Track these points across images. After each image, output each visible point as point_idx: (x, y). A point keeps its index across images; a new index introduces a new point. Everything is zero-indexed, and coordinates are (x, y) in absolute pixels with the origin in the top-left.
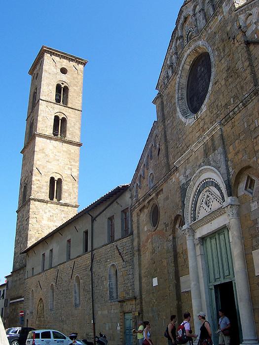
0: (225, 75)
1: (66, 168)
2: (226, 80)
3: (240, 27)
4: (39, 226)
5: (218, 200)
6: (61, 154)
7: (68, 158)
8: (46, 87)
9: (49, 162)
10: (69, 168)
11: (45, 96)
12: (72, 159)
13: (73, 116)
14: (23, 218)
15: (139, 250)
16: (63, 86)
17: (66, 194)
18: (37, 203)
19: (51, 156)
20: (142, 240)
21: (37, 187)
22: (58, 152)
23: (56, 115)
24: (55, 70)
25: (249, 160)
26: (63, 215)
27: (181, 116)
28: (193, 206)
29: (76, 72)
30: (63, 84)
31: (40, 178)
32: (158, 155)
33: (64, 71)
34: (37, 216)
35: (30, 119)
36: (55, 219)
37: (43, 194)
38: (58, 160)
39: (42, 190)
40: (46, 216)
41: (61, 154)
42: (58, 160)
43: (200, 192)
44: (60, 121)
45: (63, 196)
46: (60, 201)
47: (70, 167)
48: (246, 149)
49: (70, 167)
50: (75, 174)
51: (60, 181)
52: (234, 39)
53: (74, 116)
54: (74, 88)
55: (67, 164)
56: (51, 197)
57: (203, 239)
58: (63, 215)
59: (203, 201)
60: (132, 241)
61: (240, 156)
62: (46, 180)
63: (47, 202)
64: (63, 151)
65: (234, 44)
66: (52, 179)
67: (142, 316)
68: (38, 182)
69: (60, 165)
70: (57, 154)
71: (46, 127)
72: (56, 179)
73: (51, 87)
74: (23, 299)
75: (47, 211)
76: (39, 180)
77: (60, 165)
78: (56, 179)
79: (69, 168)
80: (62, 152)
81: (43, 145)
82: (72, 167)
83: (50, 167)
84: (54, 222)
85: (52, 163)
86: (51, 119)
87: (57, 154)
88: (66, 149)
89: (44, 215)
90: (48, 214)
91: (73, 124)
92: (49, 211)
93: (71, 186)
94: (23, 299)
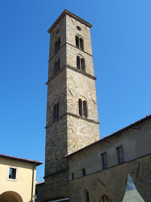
1: (88, 94)
4: (75, 136)
7: (89, 87)
8: (70, 36)
9: (77, 88)
11: (69, 41)
13: (88, 58)
14: (55, 130)
16: (79, 38)
17: (90, 113)
18: (71, 117)
21: (71, 105)
22: (82, 81)
23: (77, 55)
24: (73, 26)
26: (90, 129)
31: (72, 99)
33: (79, 28)
34: (73, 128)
35: (54, 59)
36: (85, 131)
37: (75, 111)
38: (82, 87)
40: (79, 128)
41: (84, 83)
46: (87, 118)
47: (91, 93)
49: (91, 93)
50: (95, 99)
51: (85, 103)
53: (89, 58)
54: (86, 40)
55: (88, 91)
56: (80, 113)
62: (76, 100)
63: (78, 117)
64: (85, 81)
66: (80, 100)
68: (71, 101)
69: (84, 90)
70: (81, 82)
72: (83, 100)
73: (72, 37)
74: (67, 199)
75: (79, 124)
76: (71, 100)
77: (84, 90)
78: (83, 100)
80: (84, 82)
82: (92, 94)
83: (78, 91)
84: (85, 134)
85: (79, 88)
87: (81, 82)
89: (78, 127)
91: (89, 64)
92: (81, 125)
93: (93, 107)
94: (67, 199)
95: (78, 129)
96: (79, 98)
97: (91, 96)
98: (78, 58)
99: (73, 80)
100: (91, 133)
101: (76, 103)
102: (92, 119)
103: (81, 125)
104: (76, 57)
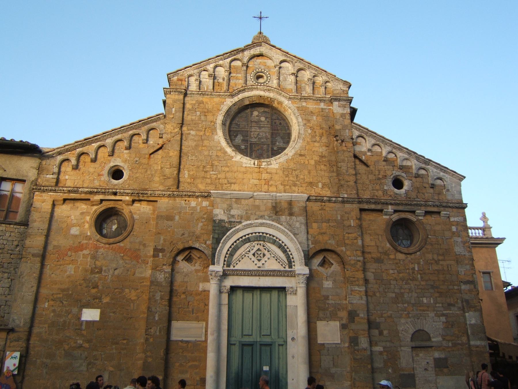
0: (317, 158)
2: (317, 163)
3: (352, 139)
5: (278, 261)
15: (43, 257)
20: (55, 243)
25: (336, 246)
27: (224, 143)
28: (230, 249)
32: (151, 154)
43: (248, 240)
48: (335, 236)
52: (343, 141)
57: (233, 289)
59: (249, 251)
60: (23, 236)
61: (326, 238)
65: (341, 145)
67: (26, 360)
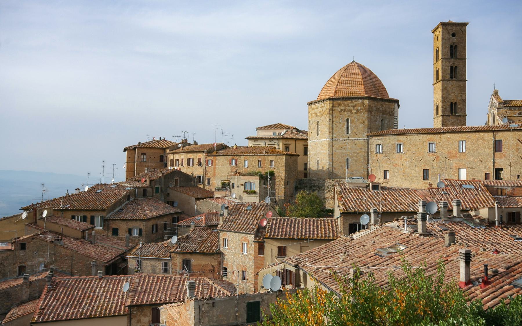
1: (459, 96)
6: (456, 89)
7: (460, 90)
10: (460, 95)
12: (462, 90)
17: (460, 110)
19: (450, 91)
22: (454, 88)
29: (462, 33)
30: (454, 44)
31: (445, 104)
38: (454, 92)
39: (447, 110)
42: (454, 92)
44: (454, 69)
45: (458, 111)
49: (461, 94)
51: (456, 103)
55: (459, 94)
56: (452, 113)
58: (458, 121)
64: (457, 86)
66: (452, 103)
68: (444, 106)
70: (453, 89)
71: (446, 75)
72: (454, 103)
75: (450, 120)
76: (445, 105)
78: (454, 103)
79: (460, 95)
81: (445, 85)
83: (450, 97)
86: (448, 69)
87: (453, 89)
88: (458, 85)
90: (451, 122)
92: (451, 120)
95: (449, 124)
96: (451, 101)
97: (461, 97)
98: (452, 67)
99: (447, 90)
100: (459, 123)
101: (448, 106)
102: (460, 114)
103: (451, 120)
104: (450, 68)
